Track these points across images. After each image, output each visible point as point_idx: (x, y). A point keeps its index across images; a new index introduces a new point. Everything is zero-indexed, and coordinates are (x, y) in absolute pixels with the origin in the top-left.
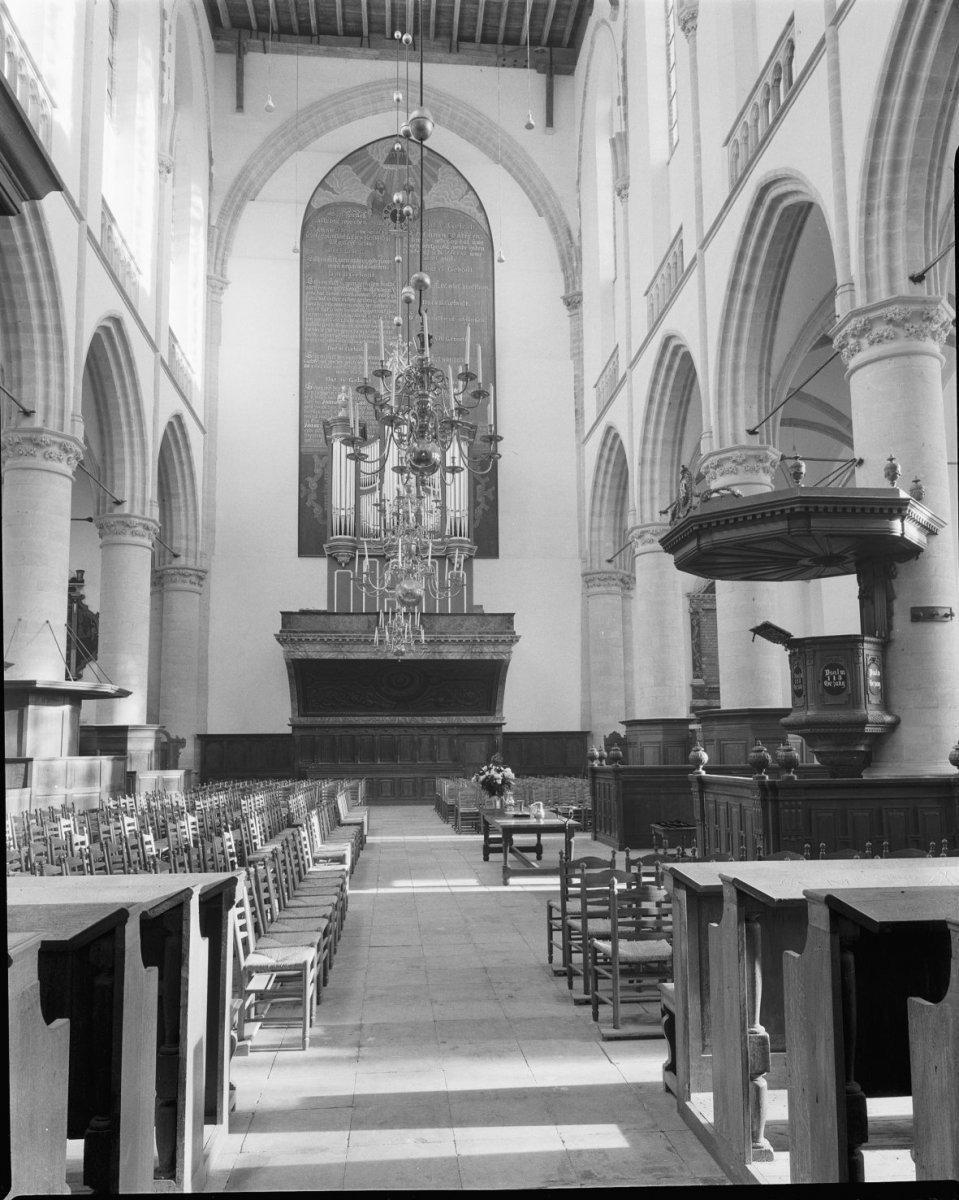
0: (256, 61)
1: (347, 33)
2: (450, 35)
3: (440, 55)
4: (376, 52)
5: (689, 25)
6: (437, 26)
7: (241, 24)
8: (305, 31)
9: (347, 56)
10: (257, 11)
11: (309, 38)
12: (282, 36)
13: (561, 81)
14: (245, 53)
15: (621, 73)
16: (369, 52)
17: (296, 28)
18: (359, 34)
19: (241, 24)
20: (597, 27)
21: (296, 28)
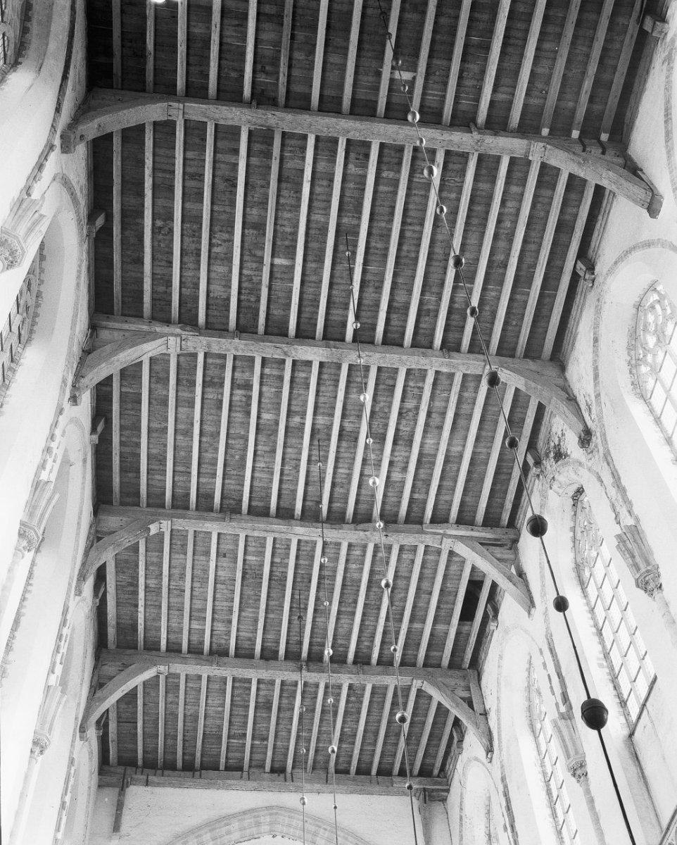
0: (138, 795)
1: (227, 768)
2: (326, 769)
3: (317, 786)
4: (255, 784)
5: (579, 772)
6: (315, 761)
7: (128, 761)
8: (189, 767)
9: (228, 788)
10: (145, 752)
11: (191, 773)
12: (166, 772)
13: (437, 808)
14: (127, 787)
15: (504, 804)
16: (251, 784)
17: (179, 764)
18: (240, 769)
19: (128, 761)
20: (469, 760)
21: (179, 764)
